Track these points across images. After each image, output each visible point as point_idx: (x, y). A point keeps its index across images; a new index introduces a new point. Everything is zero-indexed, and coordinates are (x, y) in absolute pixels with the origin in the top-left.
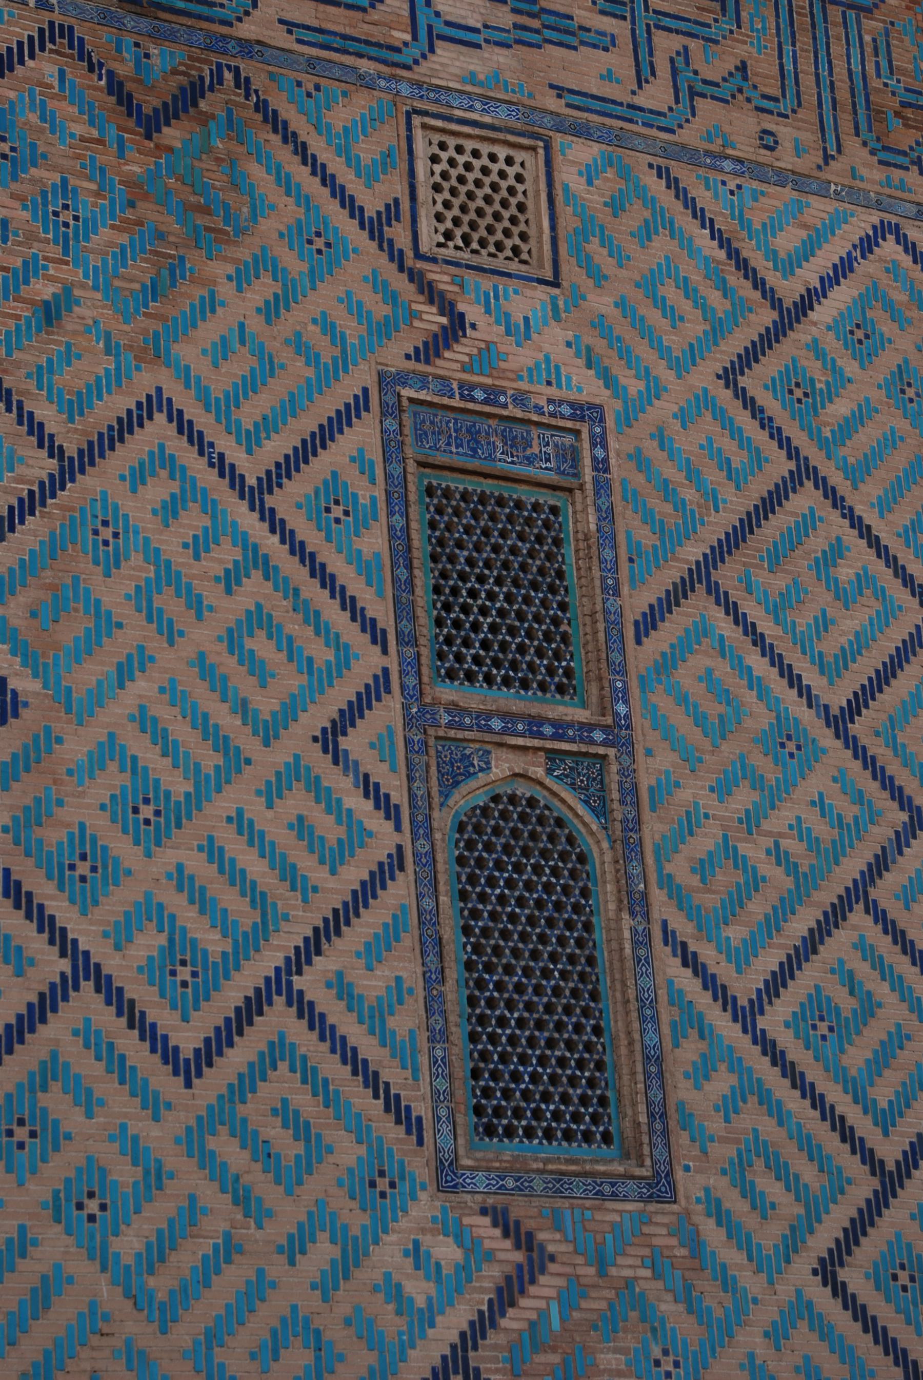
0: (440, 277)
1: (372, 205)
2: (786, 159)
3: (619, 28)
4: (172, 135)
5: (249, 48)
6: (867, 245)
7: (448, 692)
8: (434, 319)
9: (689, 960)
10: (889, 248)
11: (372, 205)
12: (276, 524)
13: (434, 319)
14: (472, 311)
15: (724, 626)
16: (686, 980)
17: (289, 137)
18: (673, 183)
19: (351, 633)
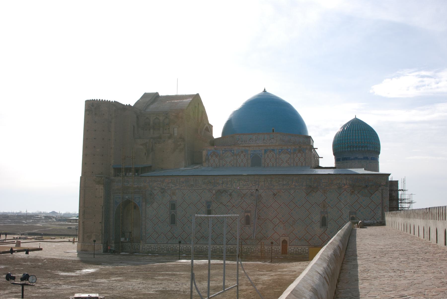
0: (171, 196)
1: (169, 194)
2: (185, 189)
3: (179, 185)
4: (163, 193)
5: (166, 190)
6: (188, 191)
7: (171, 211)
8: (171, 198)
9: (178, 219)
10: (189, 191)
11: (169, 194)
12: (166, 206)
13: (171, 198)
14: (172, 197)
15: (181, 207)
16: (177, 219)
17: (167, 193)
18: (181, 191)
19: (168, 209)
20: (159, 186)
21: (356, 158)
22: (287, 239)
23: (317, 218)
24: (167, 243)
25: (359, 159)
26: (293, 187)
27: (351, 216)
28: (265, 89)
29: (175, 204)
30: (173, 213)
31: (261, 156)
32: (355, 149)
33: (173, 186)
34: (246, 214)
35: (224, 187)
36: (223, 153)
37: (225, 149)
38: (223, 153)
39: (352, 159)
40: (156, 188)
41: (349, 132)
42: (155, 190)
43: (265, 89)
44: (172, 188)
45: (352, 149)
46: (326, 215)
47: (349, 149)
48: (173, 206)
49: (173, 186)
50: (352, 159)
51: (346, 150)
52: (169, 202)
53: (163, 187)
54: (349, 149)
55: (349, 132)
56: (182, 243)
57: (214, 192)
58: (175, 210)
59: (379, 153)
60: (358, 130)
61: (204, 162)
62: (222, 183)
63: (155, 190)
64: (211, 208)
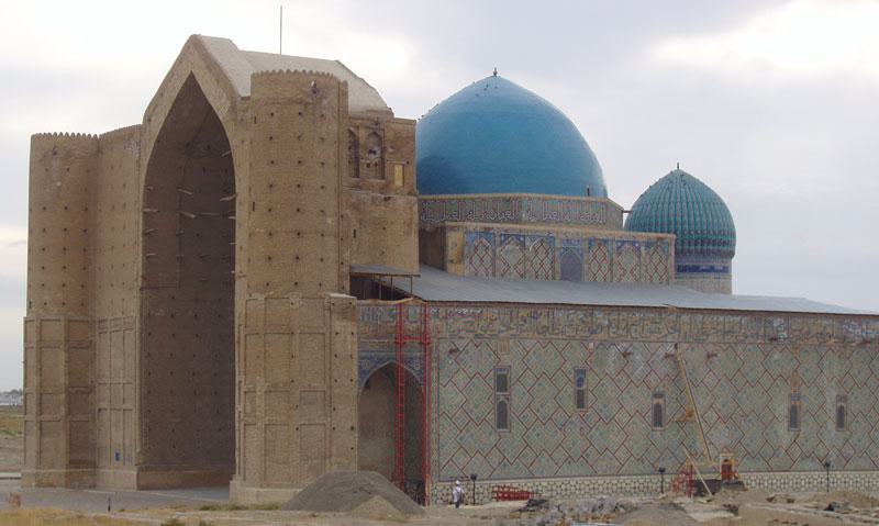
20: (471, 329)
21: (712, 269)
22: (729, 456)
23: (782, 409)
24: (489, 478)
25: (717, 271)
26: (742, 338)
27: (839, 404)
28: (495, 74)
29: (505, 376)
30: (502, 399)
31: (582, 255)
32: (711, 247)
33: (503, 328)
34: (656, 401)
35: (612, 335)
36: (501, 242)
37: (506, 231)
38: (501, 242)
39: (703, 271)
40: (463, 334)
41: (696, 205)
42: (462, 338)
43: (495, 74)
44: (501, 335)
45: (705, 248)
46: (798, 404)
47: (699, 247)
48: (502, 383)
49: (503, 328)
50: (703, 271)
51: (693, 247)
52: (492, 373)
53: (479, 332)
54: (699, 247)
55: (696, 205)
56: (667, 471)
57: (591, 345)
58: (506, 390)
59: (731, 254)
60: (693, 203)
61: (452, 261)
62: (609, 327)
63: (462, 338)
64: (584, 387)
